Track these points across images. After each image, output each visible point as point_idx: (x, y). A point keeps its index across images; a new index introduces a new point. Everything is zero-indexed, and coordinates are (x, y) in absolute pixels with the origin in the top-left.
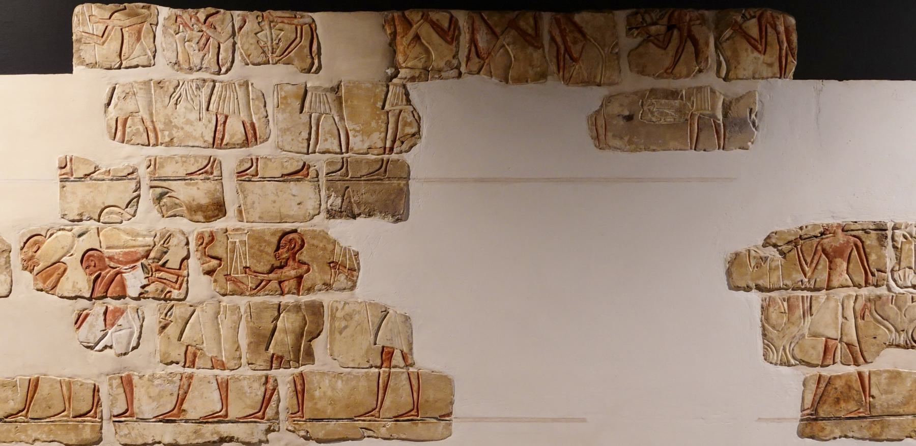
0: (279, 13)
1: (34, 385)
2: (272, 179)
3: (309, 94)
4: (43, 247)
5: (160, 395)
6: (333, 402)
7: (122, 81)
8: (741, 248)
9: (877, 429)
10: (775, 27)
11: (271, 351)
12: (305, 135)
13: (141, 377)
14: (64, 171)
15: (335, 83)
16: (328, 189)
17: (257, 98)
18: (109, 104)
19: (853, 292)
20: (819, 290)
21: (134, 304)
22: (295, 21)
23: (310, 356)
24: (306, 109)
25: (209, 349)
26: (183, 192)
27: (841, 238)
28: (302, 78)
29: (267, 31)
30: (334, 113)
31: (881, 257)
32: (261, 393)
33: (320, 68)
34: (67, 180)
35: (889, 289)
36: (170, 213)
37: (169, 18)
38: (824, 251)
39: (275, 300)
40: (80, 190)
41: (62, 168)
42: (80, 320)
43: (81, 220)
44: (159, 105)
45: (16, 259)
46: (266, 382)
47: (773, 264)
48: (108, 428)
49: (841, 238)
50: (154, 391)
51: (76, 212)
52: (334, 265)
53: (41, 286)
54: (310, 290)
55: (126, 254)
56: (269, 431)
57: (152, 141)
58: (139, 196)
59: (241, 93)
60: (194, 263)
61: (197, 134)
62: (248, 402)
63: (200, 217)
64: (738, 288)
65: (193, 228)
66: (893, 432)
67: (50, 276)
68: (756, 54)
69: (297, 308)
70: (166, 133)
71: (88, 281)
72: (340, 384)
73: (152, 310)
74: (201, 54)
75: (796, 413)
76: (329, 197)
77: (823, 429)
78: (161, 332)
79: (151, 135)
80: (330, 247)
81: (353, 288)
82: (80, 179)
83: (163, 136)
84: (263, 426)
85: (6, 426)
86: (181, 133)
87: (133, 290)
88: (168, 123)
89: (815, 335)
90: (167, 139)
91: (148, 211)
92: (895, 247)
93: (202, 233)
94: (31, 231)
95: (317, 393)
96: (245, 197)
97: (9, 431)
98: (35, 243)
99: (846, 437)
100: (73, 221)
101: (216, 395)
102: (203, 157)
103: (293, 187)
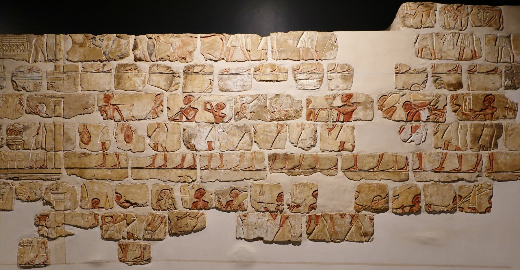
0: (487, 6)
1: (382, 156)
2: (482, 73)
3: (498, 39)
4: (387, 100)
5: (434, 161)
6: (505, 164)
7: (422, 33)
11: (480, 143)
12: (496, 55)
13: (425, 154)
14: (397, 69)
15: (508, 35)
16: (506, 77)
17: (477, 40)
18: (416, 43)
21: (423, 124)
22: (494, 9)
23: (496, 146)
24: (497, 45)
25: (454, 142)
26: (446, 78)
28: (496, 32)
29: (482, 13)
30: (508, 46)
32: (475, 161)
33: (503, 28)
34: (398, 73)
36: (440, 87)
37: (442, 7)
39: (482, 123)
40: (403, 78)
41: (396, 68)
42: (401, 130)
43: (403, 90)
44: (437, 43)
45: (376, 105)
46: (478, 156)
48: (411, 174)
50: (431, 160)
51: (402, 86)
52: (507, 109)
53: (385, 116)
54: (497, 119)
55: (421, 103)
56: (478, 176)
57: (433, 58)
58: (427, 80)
59: (470, 38)
60: (449, 108)
61: (452, 55)
62: (470, 164)
63: (452, 88)
65: (448, 93)
67: (390, 112)
69: (491, 126)
70: (440, 54)
71: (405, 114)
72: (508, 158)
73: (431, 127)
74: (455, 22)
76: (506, 81)
78: (434, 135)
79: (433, 55)
80: (506, 101)
81: (515, 118)
82: (403, 73)
83: (438, 55)
84: (476, 174)
85: (370, 173)
86: (445, 54)
87: (424, 118)
88: (440, 50)
90: (440, 57)
91: (431, 86)
93: (453, 95)
94: (379, 95)
95: (499, 161)
96: (471, 81)
97: (371, 175)
98: (384, 99)
100: (400, 90)
101: (457, 161)
102: (455, 64)
103: (491, 76)
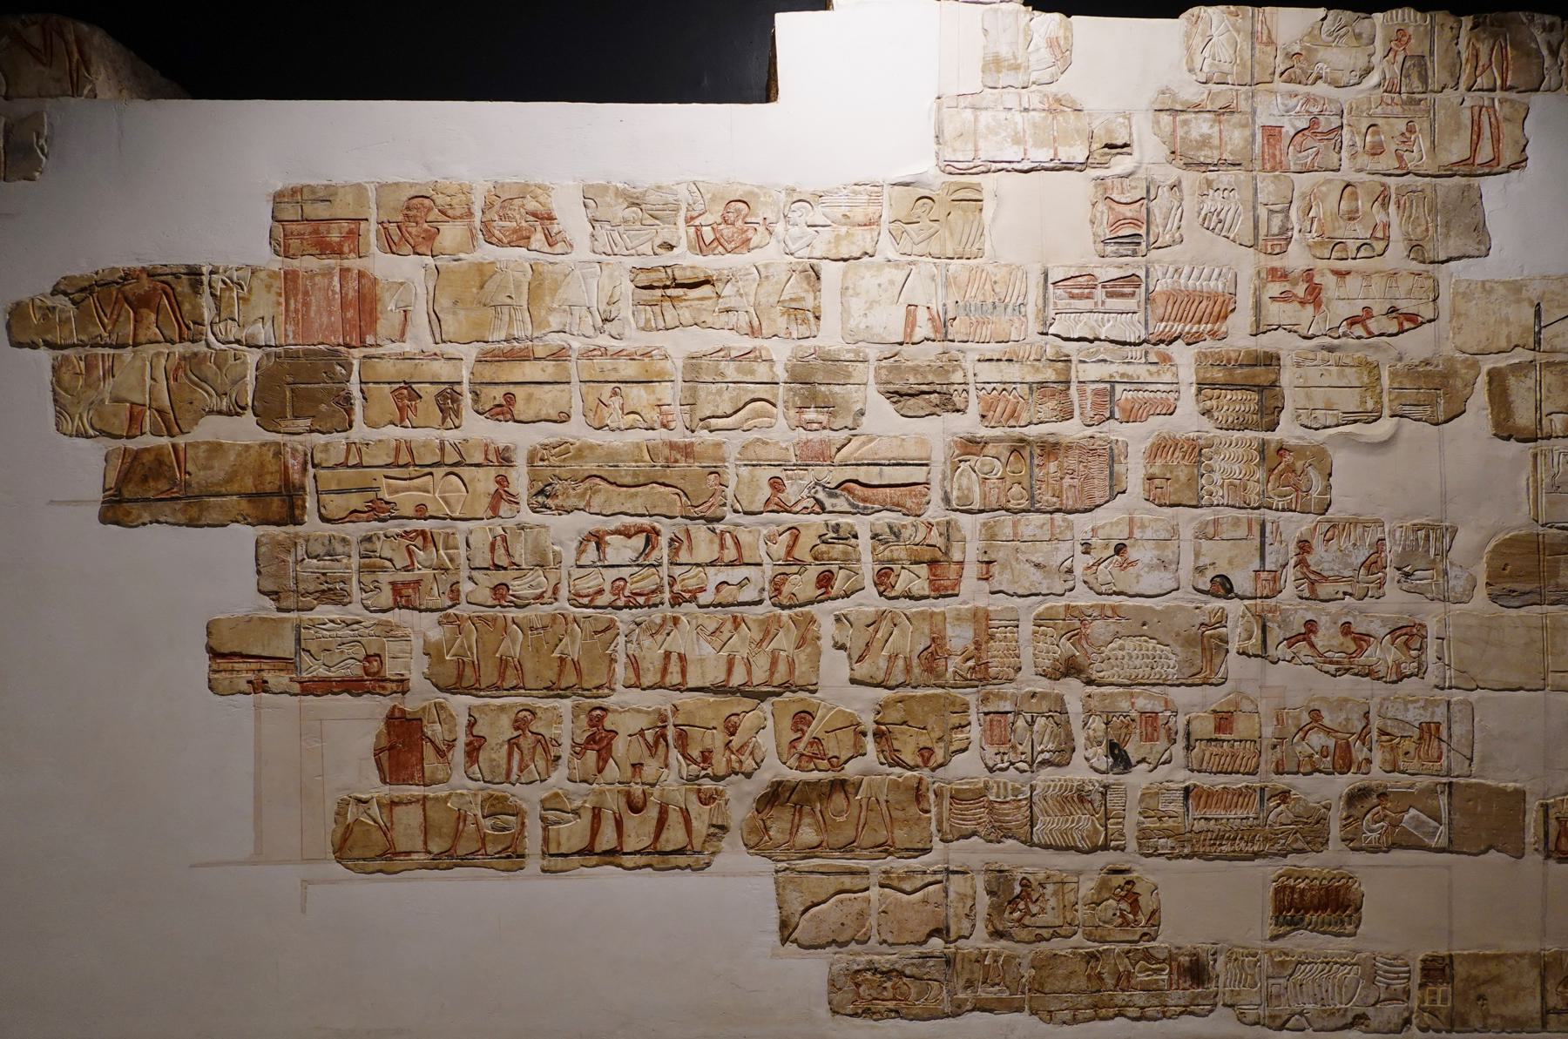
8: (24, 296)
9: (194, 512)
10: (61, 35)
19: (164, 348)
20: (124, 346)
27: (146, 284)
31: (197, 307)
35: (208, 345)
38: (126, 299)
47: (64, 316)
49: (146, 284)
64: (20, 345)
66: (214, 516)
68: (40, 67)
75: (95, 493)
77: (129, 513)
89: (117, 400)
92: (212, 295)
99: (158, 522)
